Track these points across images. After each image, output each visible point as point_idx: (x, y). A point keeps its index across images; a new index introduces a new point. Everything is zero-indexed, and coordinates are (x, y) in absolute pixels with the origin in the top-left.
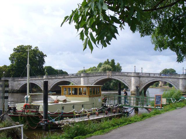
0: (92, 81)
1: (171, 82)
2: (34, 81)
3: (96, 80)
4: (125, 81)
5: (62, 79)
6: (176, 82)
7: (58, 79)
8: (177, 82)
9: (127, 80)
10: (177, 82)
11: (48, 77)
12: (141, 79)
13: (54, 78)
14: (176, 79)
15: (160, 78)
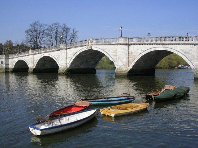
0: (71, 54)
1: (181, 52)
2: (23, 57)
3: (75, 53)
4: (109, 53)
5: (44, 54)
6: (190, 51)
7: (41, 54)
8: (191, 52)
9: (112, 51)
10: (191, 52)
11: (32, 52)
12: (131, 47)
13: (38, 53)
14: (189, 46)
15: (162, 46)
